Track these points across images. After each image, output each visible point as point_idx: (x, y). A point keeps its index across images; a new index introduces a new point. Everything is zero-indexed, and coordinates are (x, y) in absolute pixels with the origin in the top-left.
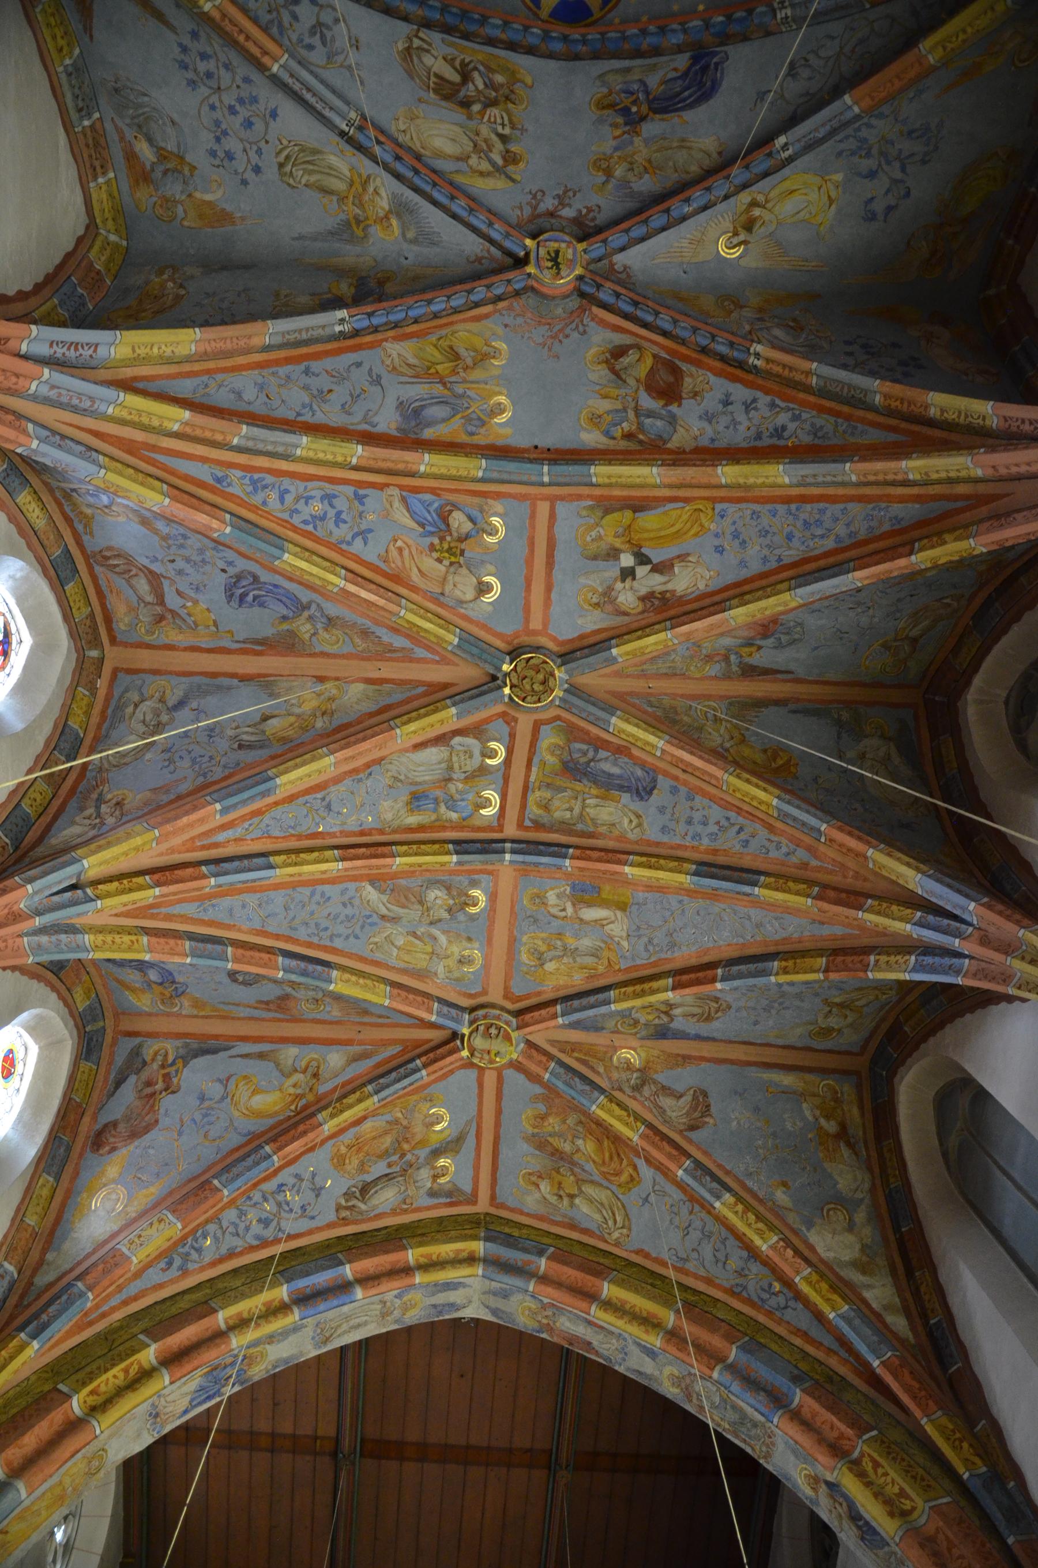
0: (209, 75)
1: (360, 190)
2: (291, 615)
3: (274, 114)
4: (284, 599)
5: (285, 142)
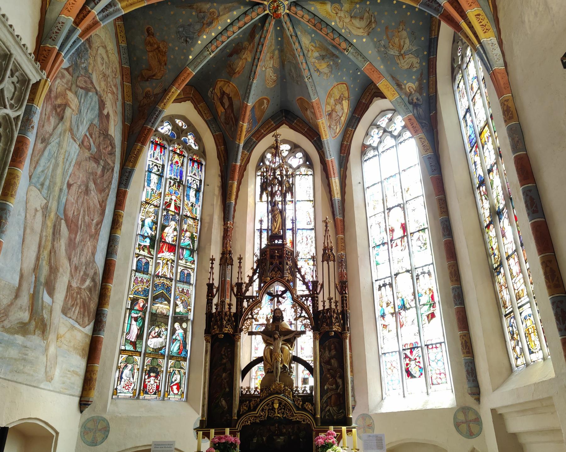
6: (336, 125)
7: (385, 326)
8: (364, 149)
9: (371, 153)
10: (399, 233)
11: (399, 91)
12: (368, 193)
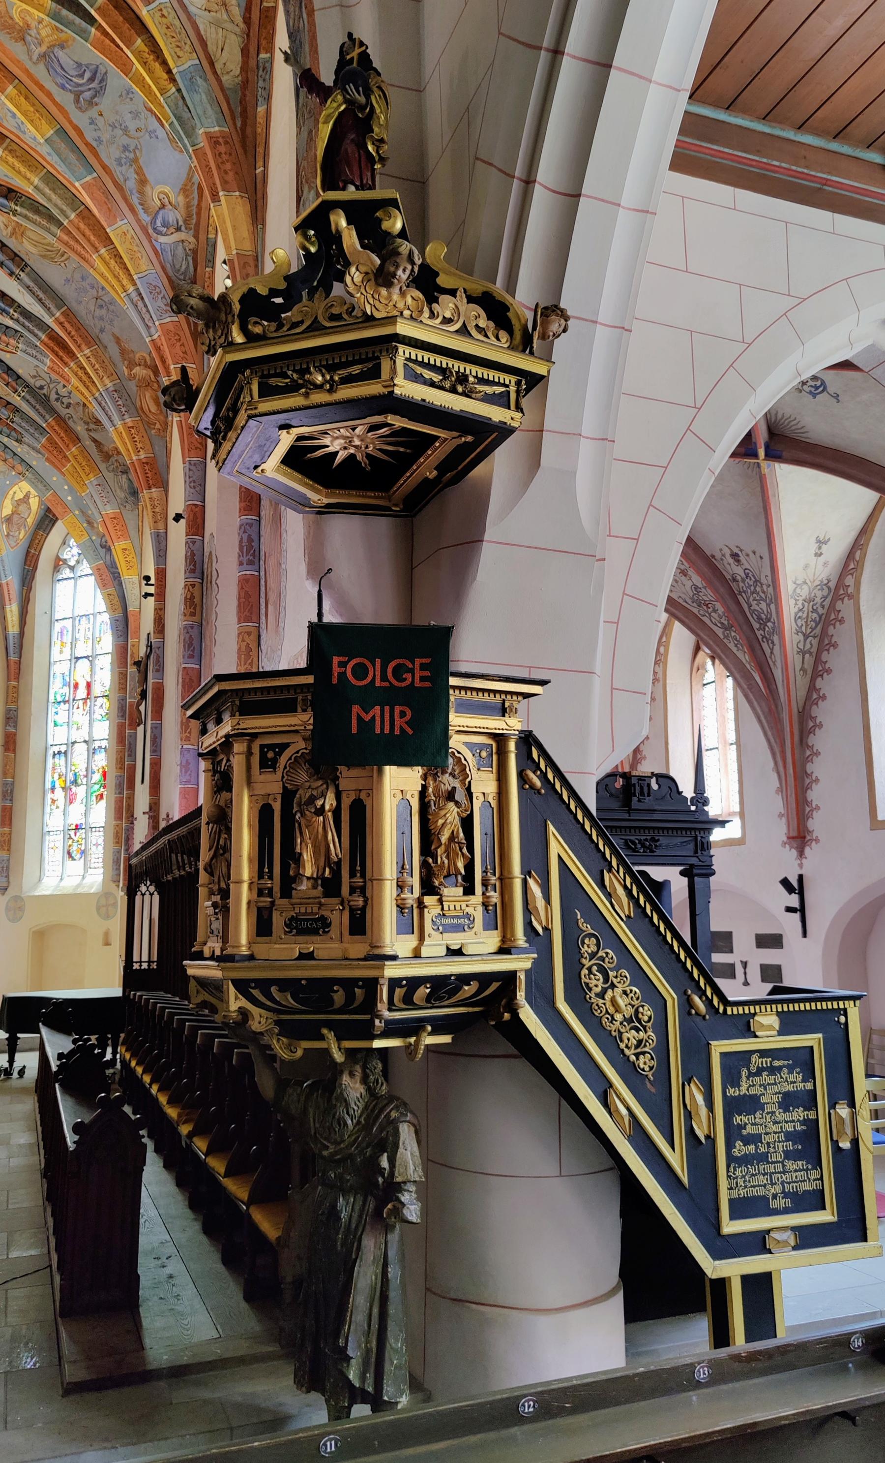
0: (101, 307)
1: (17, 230)
2: (56, 50)
3: (67, 280)
4: (59, 70)
5: (62, 264)
6: (19, 530)
7: (53, 801)
8: (58, 564)
9: (67, 573)
10: (82, 693)
11: (90, 531)
12: (57, 627)
